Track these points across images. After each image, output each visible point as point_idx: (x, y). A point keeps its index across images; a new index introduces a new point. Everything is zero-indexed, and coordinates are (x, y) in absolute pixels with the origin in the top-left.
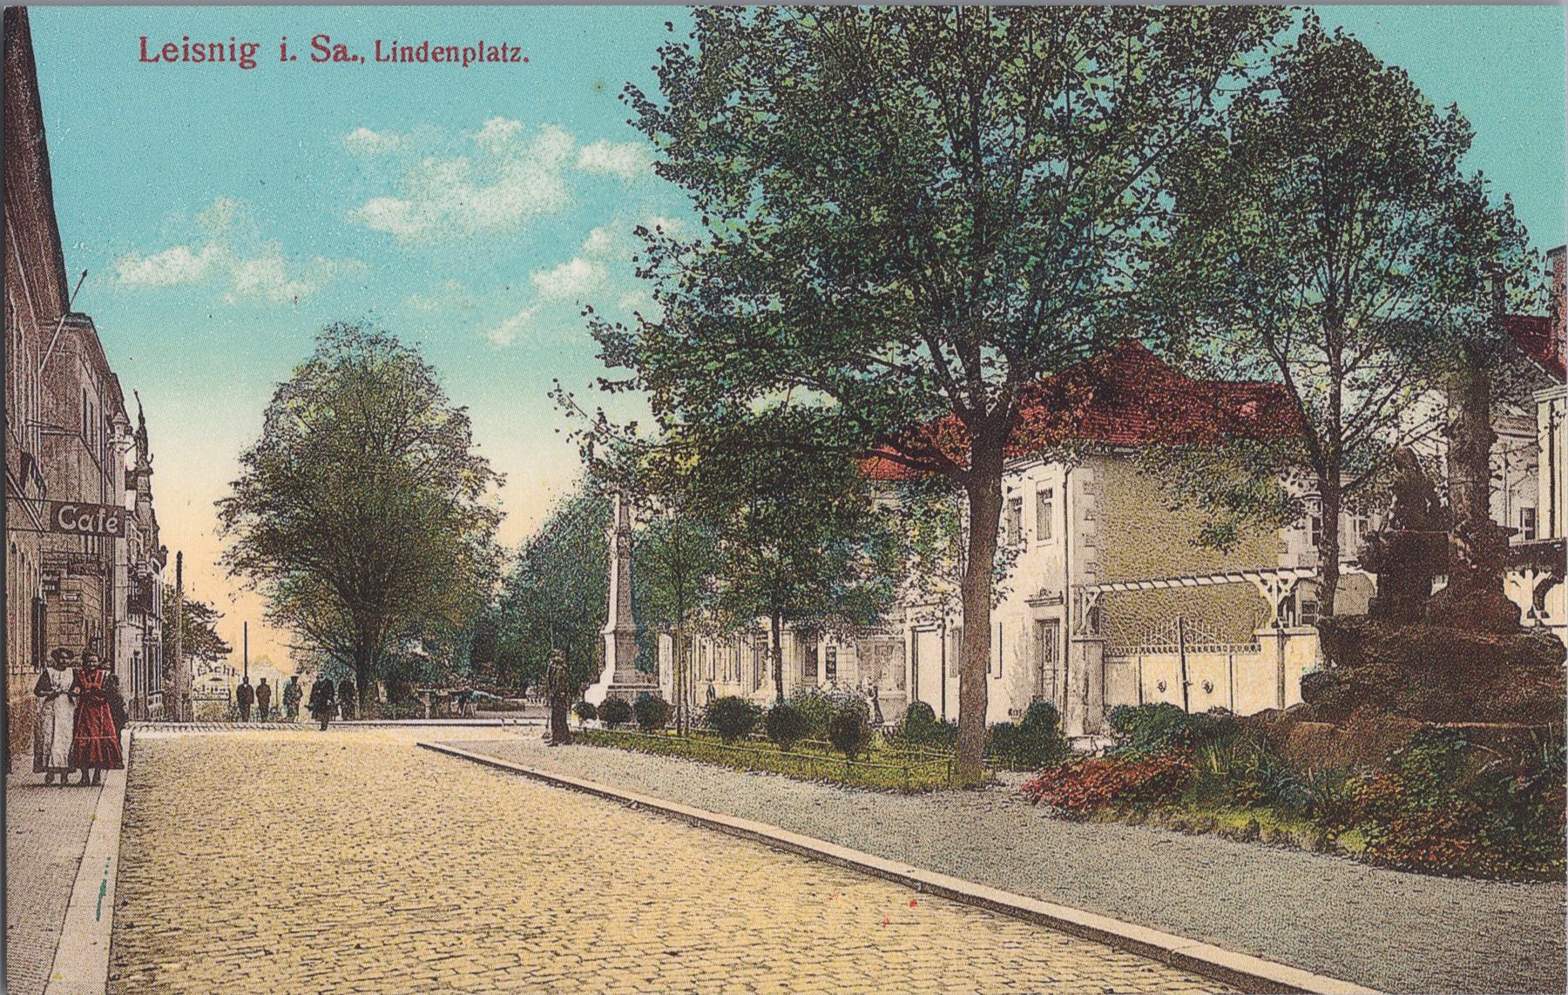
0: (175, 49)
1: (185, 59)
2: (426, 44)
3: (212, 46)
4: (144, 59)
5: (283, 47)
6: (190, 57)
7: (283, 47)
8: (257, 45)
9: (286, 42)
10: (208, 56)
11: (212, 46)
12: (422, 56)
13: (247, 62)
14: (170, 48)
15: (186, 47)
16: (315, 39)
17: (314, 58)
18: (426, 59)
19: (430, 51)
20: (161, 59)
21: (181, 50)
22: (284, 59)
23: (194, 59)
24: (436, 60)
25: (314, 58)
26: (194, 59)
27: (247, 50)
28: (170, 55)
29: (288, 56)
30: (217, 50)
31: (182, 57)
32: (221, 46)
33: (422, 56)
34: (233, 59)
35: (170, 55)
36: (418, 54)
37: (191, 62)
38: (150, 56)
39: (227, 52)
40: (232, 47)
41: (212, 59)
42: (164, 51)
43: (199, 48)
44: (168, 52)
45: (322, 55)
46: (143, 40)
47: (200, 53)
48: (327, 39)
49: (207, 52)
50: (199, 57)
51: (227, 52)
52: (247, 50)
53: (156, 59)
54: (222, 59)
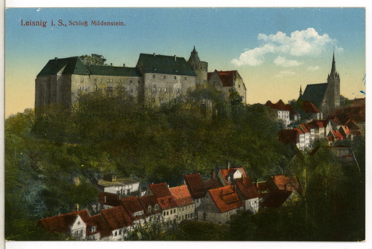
0: (29, 23)
1: (31, 25)
2: (103, 21)
3: (37, 22)
5: (52, 22)
6: (32, 25)
7: (52, 22)
8: (47, 22)
9: (53, 21)
10: (36, 25)
11: (37, 22)
12: (102, 24)
13: (44, 26)
14: (27, 22)
15: (30, 22)
16: (59, 21)
18: (103, 25)
19: (104, 23)
20: (26, 25)
21: (30, 23)
22: (52, 25)
23: (33, 25)
24: (105, 25)
26: (33, 25)
27: (44, 23)
28: (28, 24)
29: (53, 24)
30: (38, 23)
31: (30, 25)
32: (38, 22)
33: (102, 24)
34: (41, 25)
35: (28, 24)
36: (101, 24)
37: (32, 26)
39: (40, 24)
40: (41, 22)
42: (26, 23)
43: (34, 23)
44: (27, 23)
46: (22, 21)
47: (34, 24)
49: (35, 23)
50: (34, 24)
52: (44, 23)
53: (25, 25)
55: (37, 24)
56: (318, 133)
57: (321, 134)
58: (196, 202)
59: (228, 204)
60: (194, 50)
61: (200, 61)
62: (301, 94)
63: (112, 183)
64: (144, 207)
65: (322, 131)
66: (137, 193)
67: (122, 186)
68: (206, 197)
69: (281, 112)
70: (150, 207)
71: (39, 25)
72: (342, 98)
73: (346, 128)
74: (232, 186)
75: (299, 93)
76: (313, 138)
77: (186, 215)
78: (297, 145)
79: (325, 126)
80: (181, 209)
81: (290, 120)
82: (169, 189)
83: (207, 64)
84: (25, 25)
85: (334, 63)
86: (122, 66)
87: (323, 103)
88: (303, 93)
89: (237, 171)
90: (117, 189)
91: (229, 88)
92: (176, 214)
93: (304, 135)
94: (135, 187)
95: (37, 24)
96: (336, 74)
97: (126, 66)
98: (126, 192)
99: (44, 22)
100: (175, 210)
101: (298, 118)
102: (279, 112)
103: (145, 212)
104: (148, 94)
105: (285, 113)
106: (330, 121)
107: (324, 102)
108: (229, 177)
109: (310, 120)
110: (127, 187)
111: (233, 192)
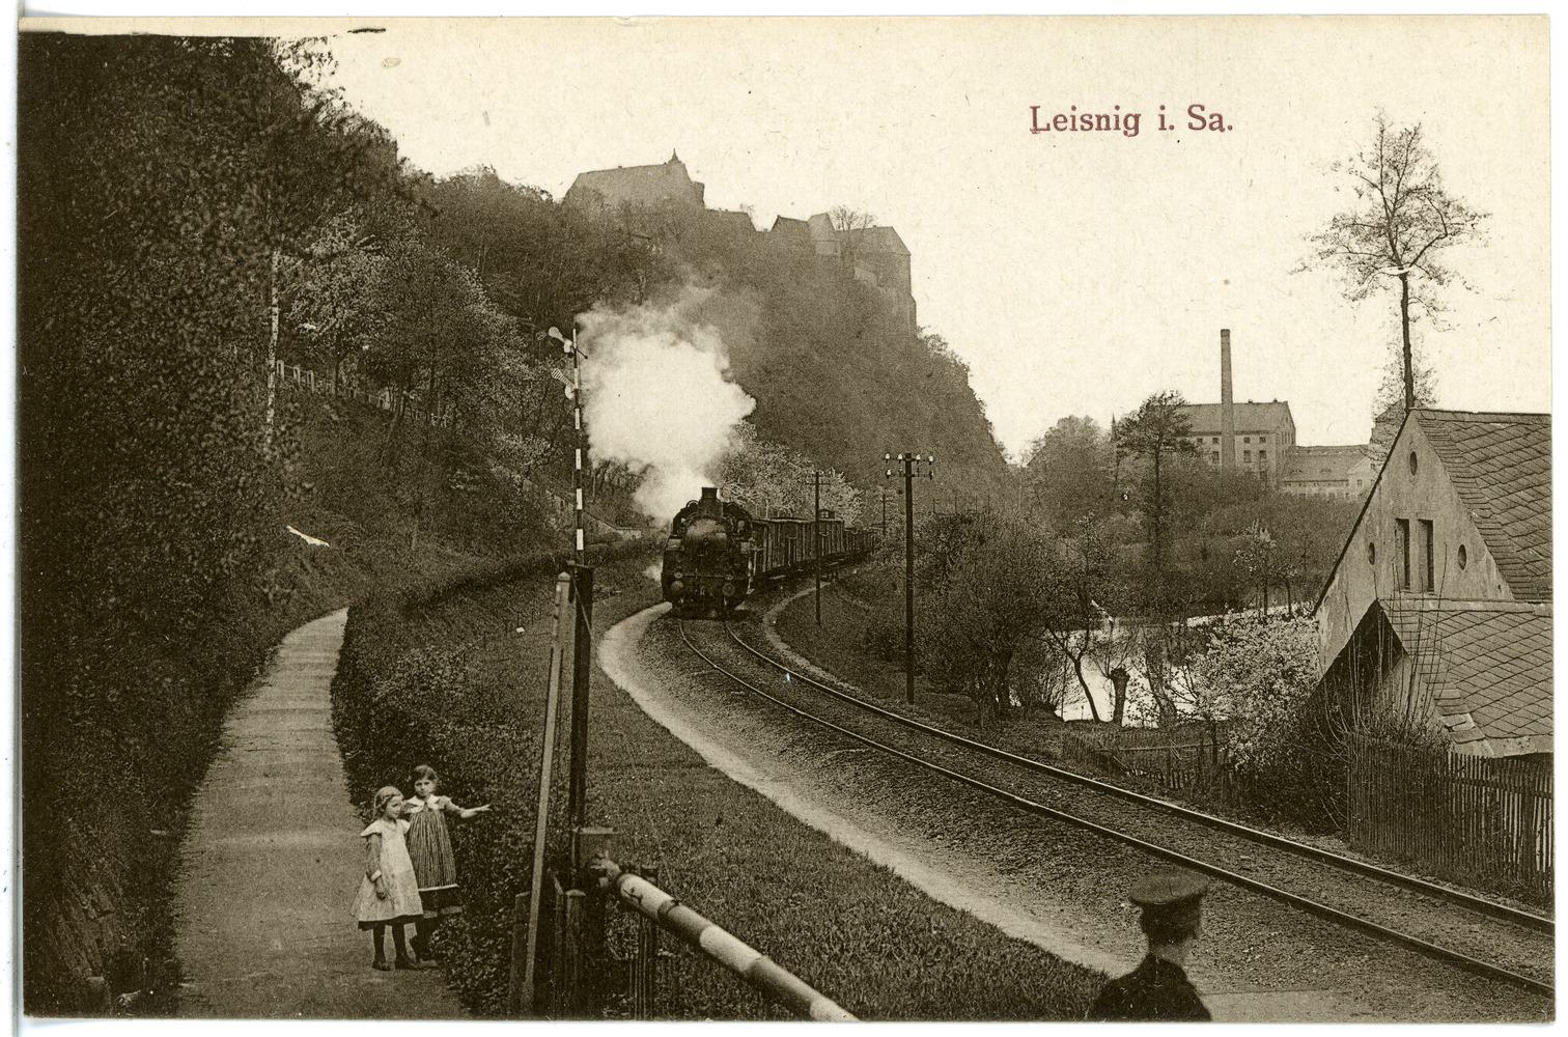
0: (1066, 121)
3: (1099, 118)
4: (1035, 130)
5: (1162, 117)
6: (1078, 126)
7: (1162, 117)
10: (1095, 125)
11: (1099, 118)
17: (1191, 126)
20: (1052, 126)
21: (1070, 120)
22: (1163, 128)
25: (1191, 126)
26: (1082, 128)
29: (1167, 125)
34: (1117, 128)
38: (1039, 126)
39: (1112, 124)
40: (1117, 117)
41: (1099, 128)
42: (1055, 121)
45: (1199, 124)
46: (1035, 109)
48: (1203, 108)
49: (1094, 121)
50: (1087, 126)
51: (1112, 124)
54: (1108, 128)
55: (1099, 124)
71: (1108, 128)
84: (1048, 129)
95: (1099, 124)
99: (1130, 115)
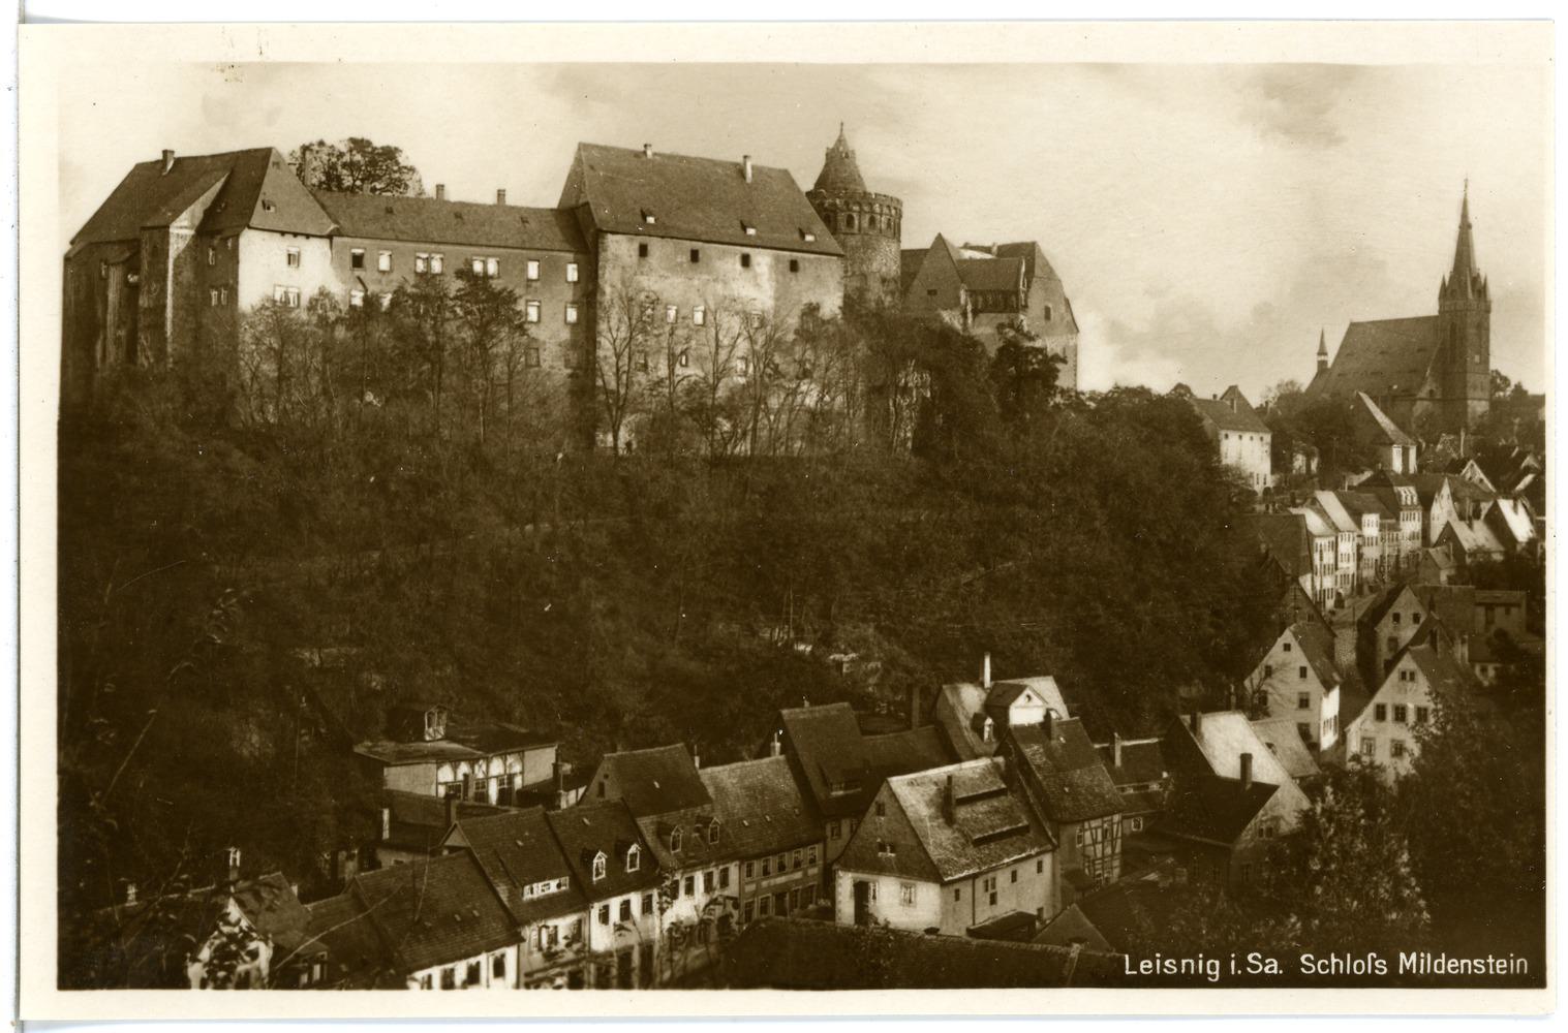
56: (1395, 533)
57: (1413, 537)
58: (829, 833)
59: (978, 843)
60: (840, 141)
61: (866, 194)
62: (1322, 364)
63: (425, 744)
64: (575, 861)
65: (1411, 526)
66: (541, 795)
67: (473, 761)
68: (873, 809)
69: (1234, 437)
70: (600, 860)
72: (1498, 381)
73: (1515, 508)
74: (1000, 760)
75: (1316, 356)
76: (1372, 553)
77: (780, 896)
78: (1306, 582)
79: (1426, 502)
80: (757, 866)
81: (1273, 473)
82: (700, 772)
83: (899, 207)
85: (1465, 227)
86: (490, 199)
87: (1419, 403)
88: (1330, 359)
89: (1027, 691)
90: (446, 774)
91: (1004, 318)
92: (733, 890)
93: (1333, 539)
94: (538, 765)
96: (1475, 279)
97: (510, 201)
98: (493, 791)
100: (725, 875)
101: (1308, 466)
102: (1227, 436)
103: (575, 881)
104: (612, 332)
105: (1252, 438)
106: (1446, 480)
107: (1422, 399)
108: (989, 721)
109: (1363, 472)
110: (497, 767)
111: (1003, 786)
